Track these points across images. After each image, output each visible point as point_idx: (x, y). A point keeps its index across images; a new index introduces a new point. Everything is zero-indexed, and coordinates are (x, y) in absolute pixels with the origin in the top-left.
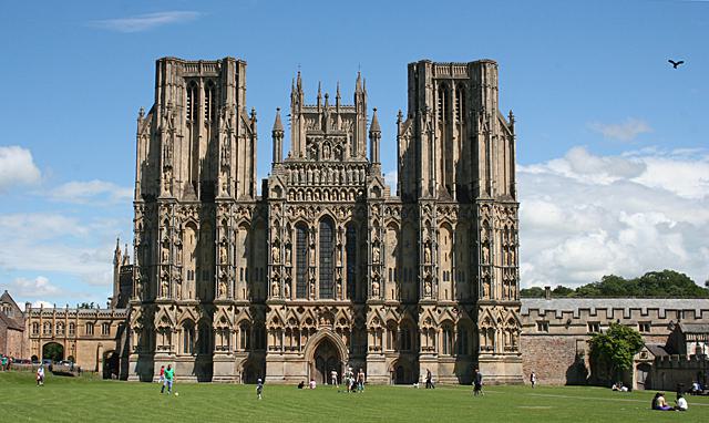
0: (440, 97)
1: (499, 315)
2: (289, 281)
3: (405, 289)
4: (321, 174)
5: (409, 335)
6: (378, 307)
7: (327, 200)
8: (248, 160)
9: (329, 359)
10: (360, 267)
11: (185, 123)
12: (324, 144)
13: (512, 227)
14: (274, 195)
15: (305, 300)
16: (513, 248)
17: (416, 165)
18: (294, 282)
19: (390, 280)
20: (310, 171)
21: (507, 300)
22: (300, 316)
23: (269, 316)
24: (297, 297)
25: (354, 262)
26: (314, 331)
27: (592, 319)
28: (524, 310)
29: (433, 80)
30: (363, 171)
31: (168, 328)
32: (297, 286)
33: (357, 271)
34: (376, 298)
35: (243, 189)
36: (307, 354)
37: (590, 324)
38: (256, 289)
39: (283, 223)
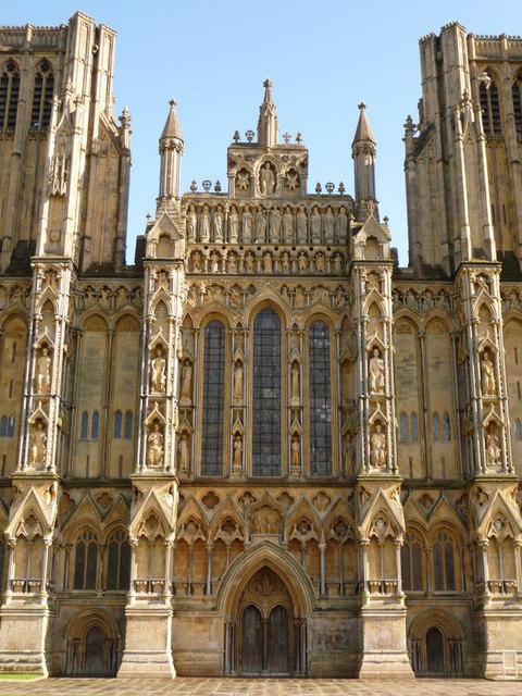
4: (254, 223)
5: (449, 554)
7: (269, 270)
8: (112, 199)
9: (274, 611)
10: (340, 408)
12: (263, 167)
14: (151, 251)
17: (448, 209)
18: (198, 438)
20: (234, 217)
23: (138, 515)
25: (327, 398)
26: (238, 543)
29: (470, 62)
30: (343, 216)
32: (205, 448)
33: (333, 416)
35: (99, 252)
38: (114, 454)
39: (177, 310)
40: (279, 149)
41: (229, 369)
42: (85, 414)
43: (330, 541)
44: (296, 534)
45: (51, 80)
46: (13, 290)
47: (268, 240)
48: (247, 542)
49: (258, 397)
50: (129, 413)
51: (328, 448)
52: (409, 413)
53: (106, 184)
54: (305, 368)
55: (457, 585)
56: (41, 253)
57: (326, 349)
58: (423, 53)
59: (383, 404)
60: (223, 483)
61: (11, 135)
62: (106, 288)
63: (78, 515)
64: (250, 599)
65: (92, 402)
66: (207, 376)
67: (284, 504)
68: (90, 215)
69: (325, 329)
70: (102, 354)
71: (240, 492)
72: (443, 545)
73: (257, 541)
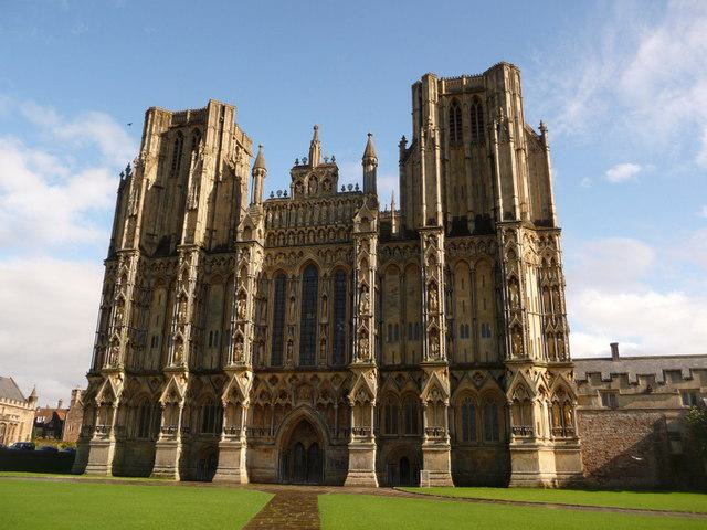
0: (452, 117)
1: (540, 382)
3: (410, 353)
8: (229, 207)
13: (554, 260)
16: (556, 288)
18: (269, 344)
19: (390, 339)
20: (293, 211)
25: (343, 317)
26: (288, 405)
27: (686, 386)
28: (579, 374)
32: (273, 350)
36: (279, 439)
37: (684, 393)
40: (321, 167)
41: (287, 303)
42: (211, 333)
44: (321, 400)
47: (312, 223)
48: (293, 404)
49: (304, 318)
51: (343, 348)
52: (394, 325)
54: (331, 300)
56: (183, 243)
57: (344, 287)
58: (413, 93)
59: (367, 321)
60: (282, 372)
62: (223, 259)
63: (204, 391)
66: (276, 308)
68: (216, 217)
70: (221, 297)
71: (290, 375)
73: (299, 404)
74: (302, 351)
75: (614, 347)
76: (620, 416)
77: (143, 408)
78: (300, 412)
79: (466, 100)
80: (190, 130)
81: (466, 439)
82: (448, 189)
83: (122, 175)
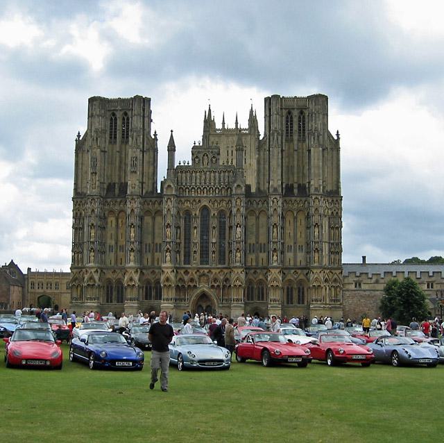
0: (287, 121)
2: (178, 252)
6: (240, 270)
7: (205, 195)
8: (152, 168)
10: (229, 243)
11: (107, 141)
15: (190, 266)
18: (182, 253)
19: (250, 251)
21: (332, 266)
22: (186, 278)
23: (163, 278)
24: (185, 264)
25: (225, 239)
26: (195, 286)
30: (231, 174)
31: (93, 285)
32: (185, 256)
33: (227, 245)
34: (238, 264)
35: (148, 188)
39: (173, 211)
41: (192, 229)
42: (146, 245)
43: (224, 286)
44: (213, 283)
45: (128, 119)
46: (120, 203)
50: (160, 244)
53: (149, 162)
55: (265, 299)
61: (115, 142)
62: (151, 201)
64: (199, 303)
65: (148, 240)
66: (185, 232)
67: (209, 275)
69: (225, 215)
70: (151, 224)
71: (196, 270)
72: (261, 287)
74: (201, 257)
75: (364, 258)
76: (362, 293)
77: (108, 287)
78: (202, 289)
79: (296, 113)
80: (122, 113)
81: (288, 303)
82: (284, 168)
83: (76, 140)
